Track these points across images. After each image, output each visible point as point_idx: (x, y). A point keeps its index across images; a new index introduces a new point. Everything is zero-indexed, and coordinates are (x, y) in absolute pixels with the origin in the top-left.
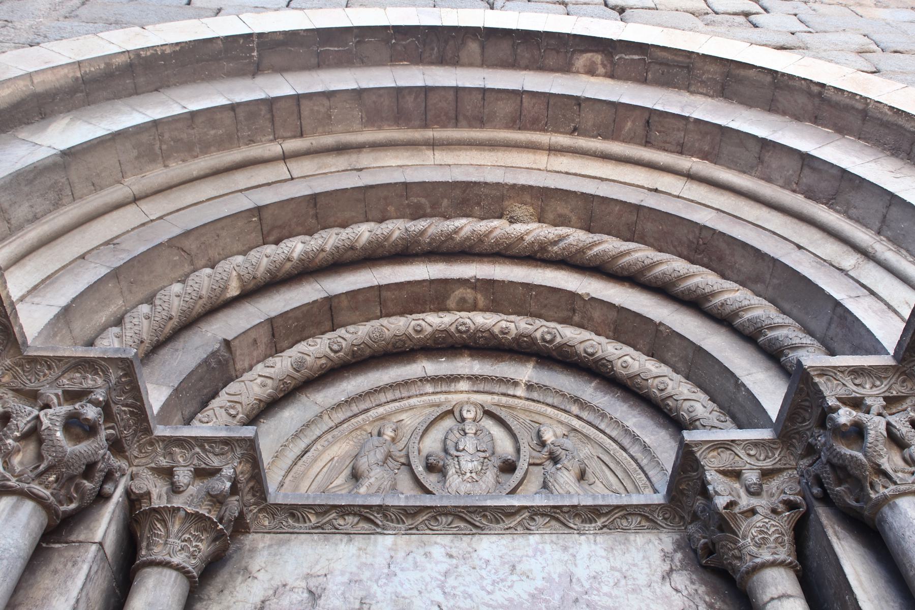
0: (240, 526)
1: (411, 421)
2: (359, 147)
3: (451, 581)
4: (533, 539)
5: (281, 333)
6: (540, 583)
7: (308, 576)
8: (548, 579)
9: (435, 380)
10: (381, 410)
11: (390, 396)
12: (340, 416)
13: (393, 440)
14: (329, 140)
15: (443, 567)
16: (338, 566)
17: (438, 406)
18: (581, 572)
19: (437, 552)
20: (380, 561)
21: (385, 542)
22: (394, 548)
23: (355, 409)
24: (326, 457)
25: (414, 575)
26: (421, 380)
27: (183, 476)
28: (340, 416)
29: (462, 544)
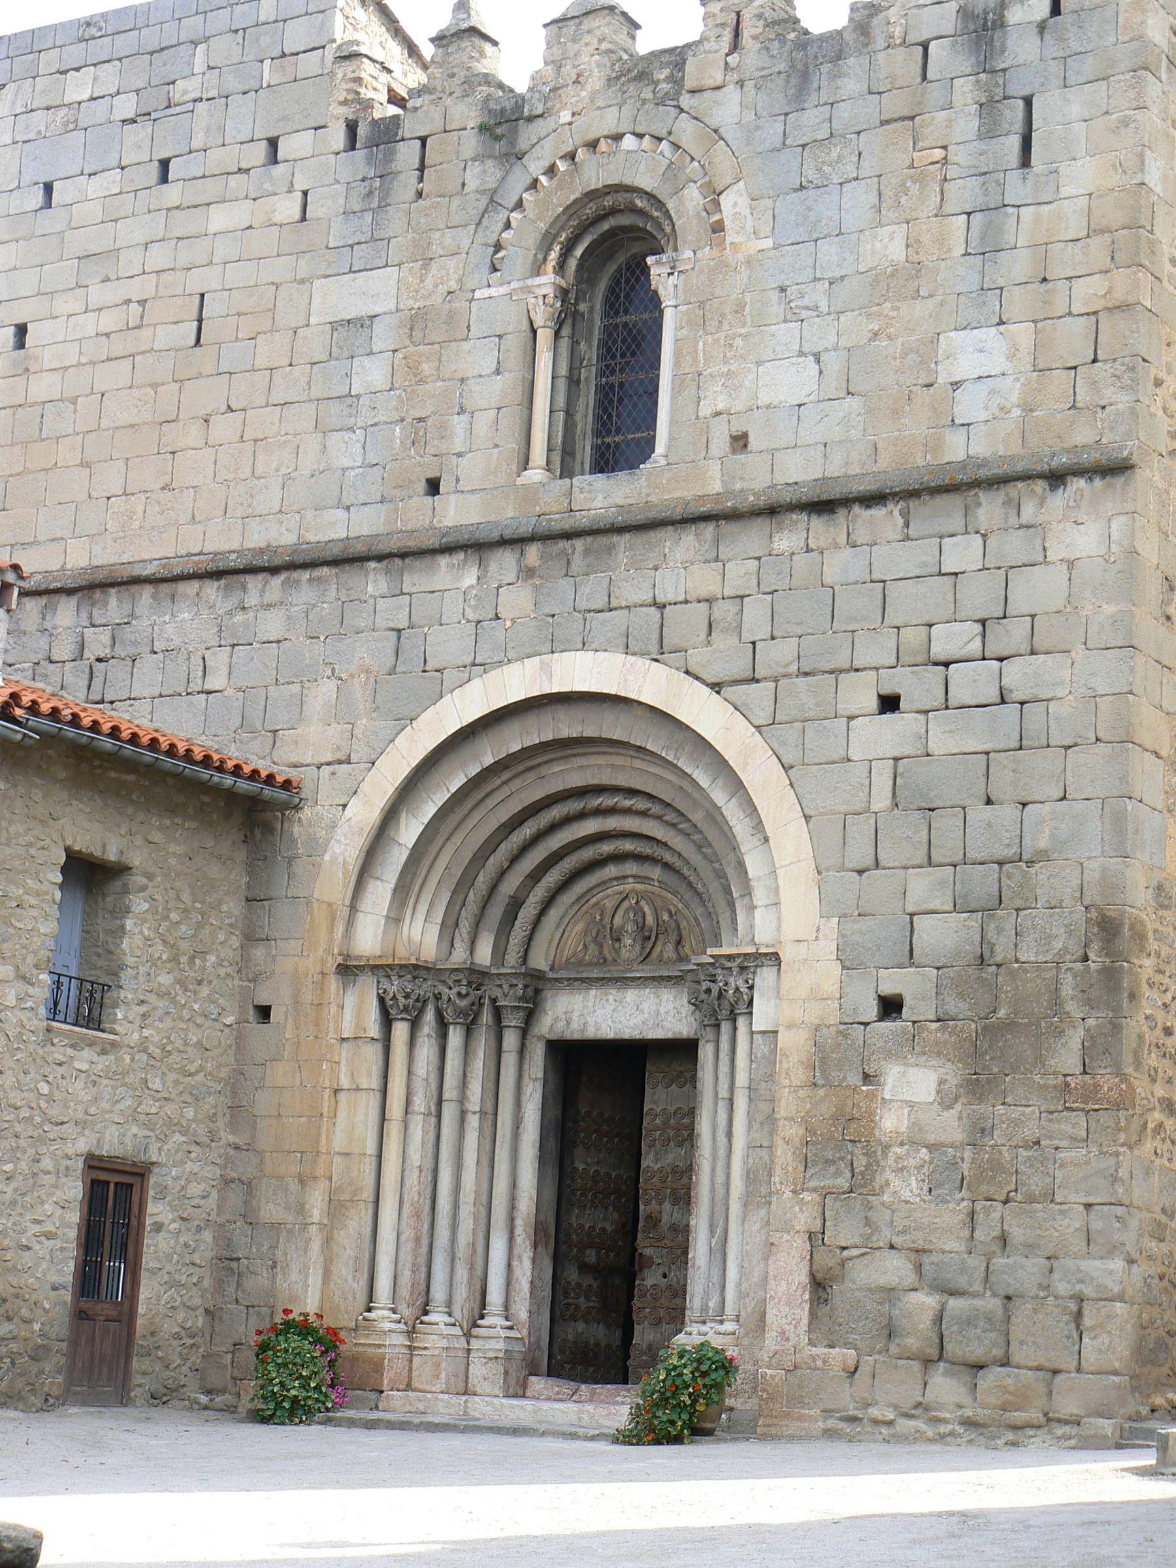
0: (537, 992)
1: (609, 904)
2: (539, 765)
3: (615, 1015)
4: (647, 991)
5: (536, 876)
6: (646, 1016)
7: (566, 1013)
8: (649, 1014)
9: (617, 879)
10: (595, 899)
11: (597, 890)
12: (576, 908)
13: (601, 920)
14: (521, 767)
15: (612, 1007)
16: (576, 1007)
17: (621, 893)
18: (662, 1010)
19: (611, 998)
20: (590, 1004)
21: (593, 992)
22: (595, 997)
23: (583, 902)
24: (573, 934)
25: (602, 1011)
26: (611, 880)
27: (506, 987)
28: (576, 908)
29: (620, 995)
